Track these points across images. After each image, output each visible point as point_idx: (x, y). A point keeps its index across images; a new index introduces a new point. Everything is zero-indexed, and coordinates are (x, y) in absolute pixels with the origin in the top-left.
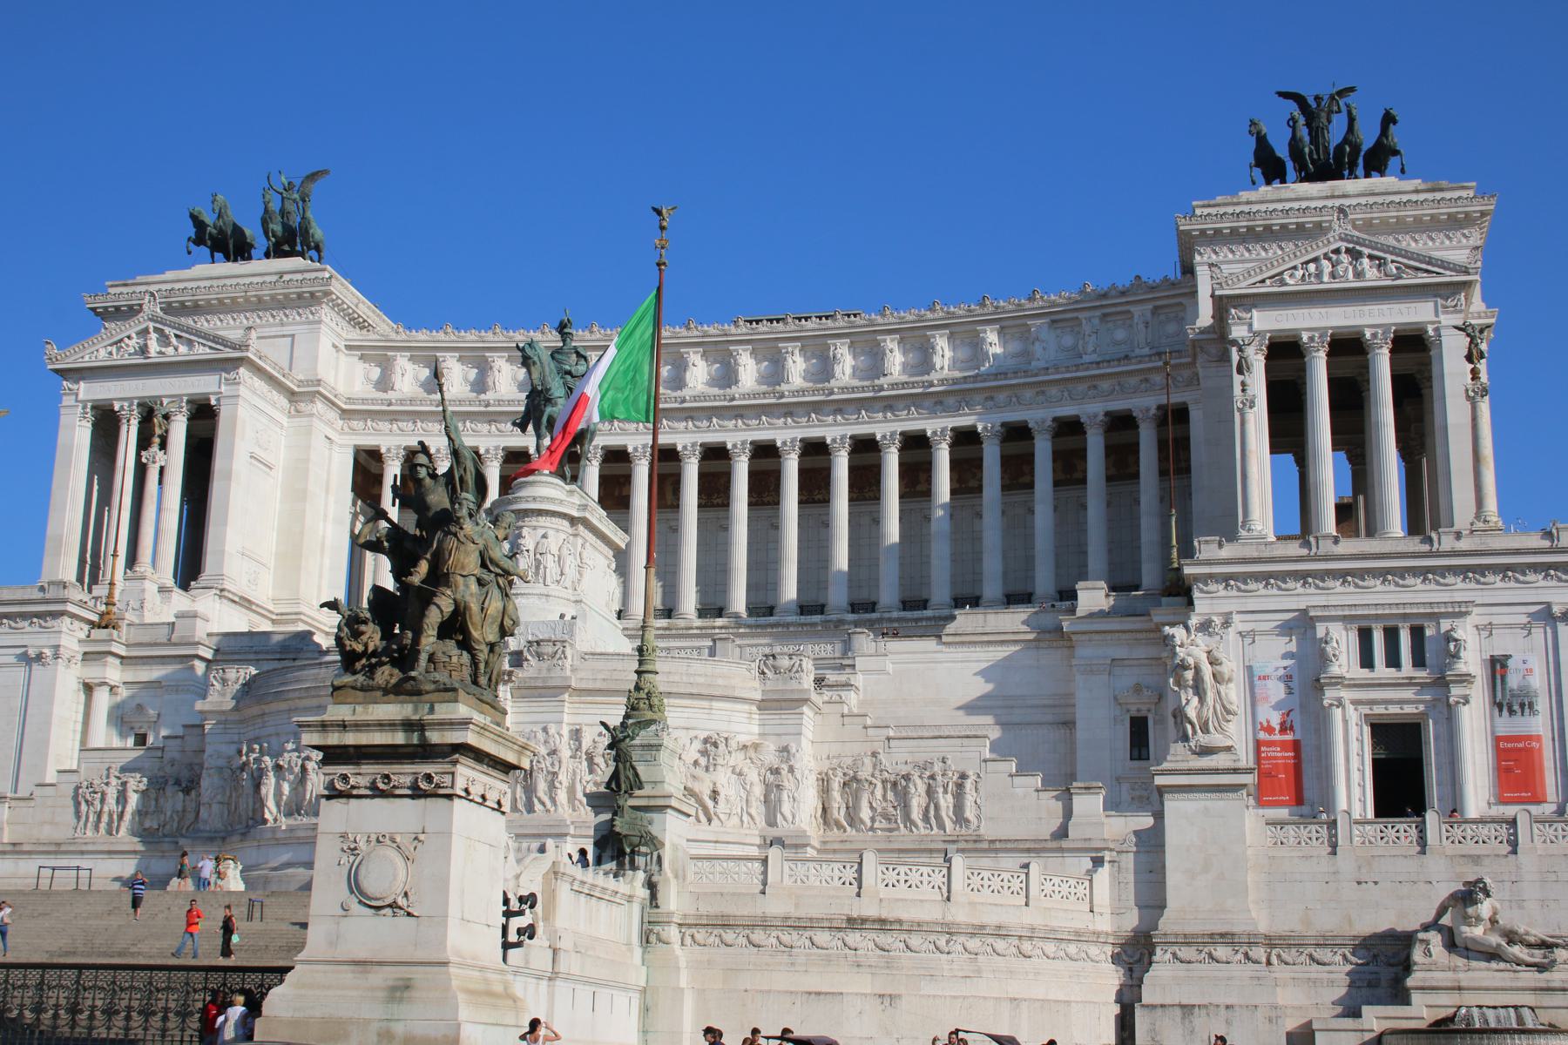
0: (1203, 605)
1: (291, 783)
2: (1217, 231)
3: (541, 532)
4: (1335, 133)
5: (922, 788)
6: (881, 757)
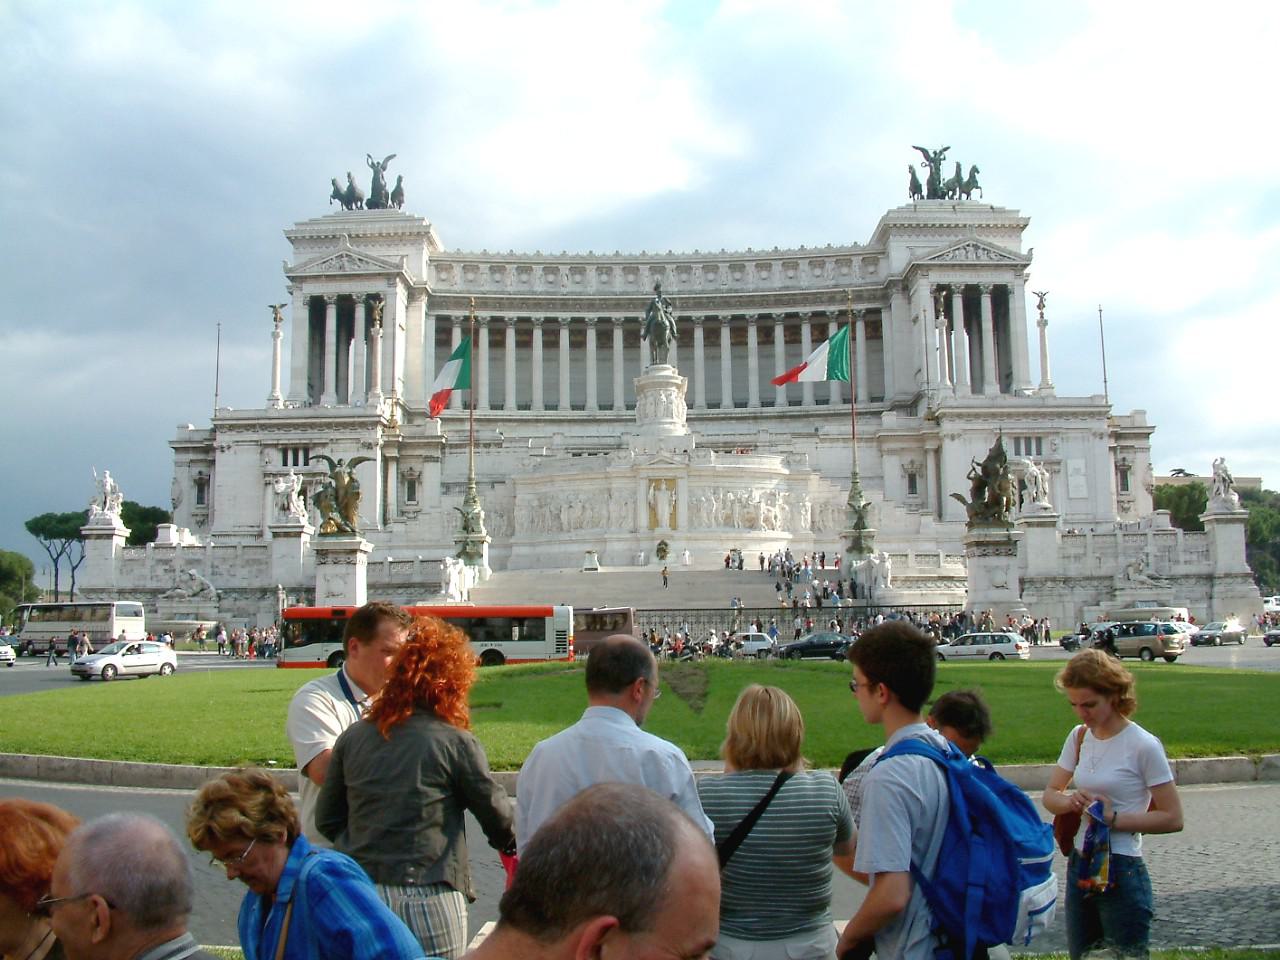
4: (947, 173)
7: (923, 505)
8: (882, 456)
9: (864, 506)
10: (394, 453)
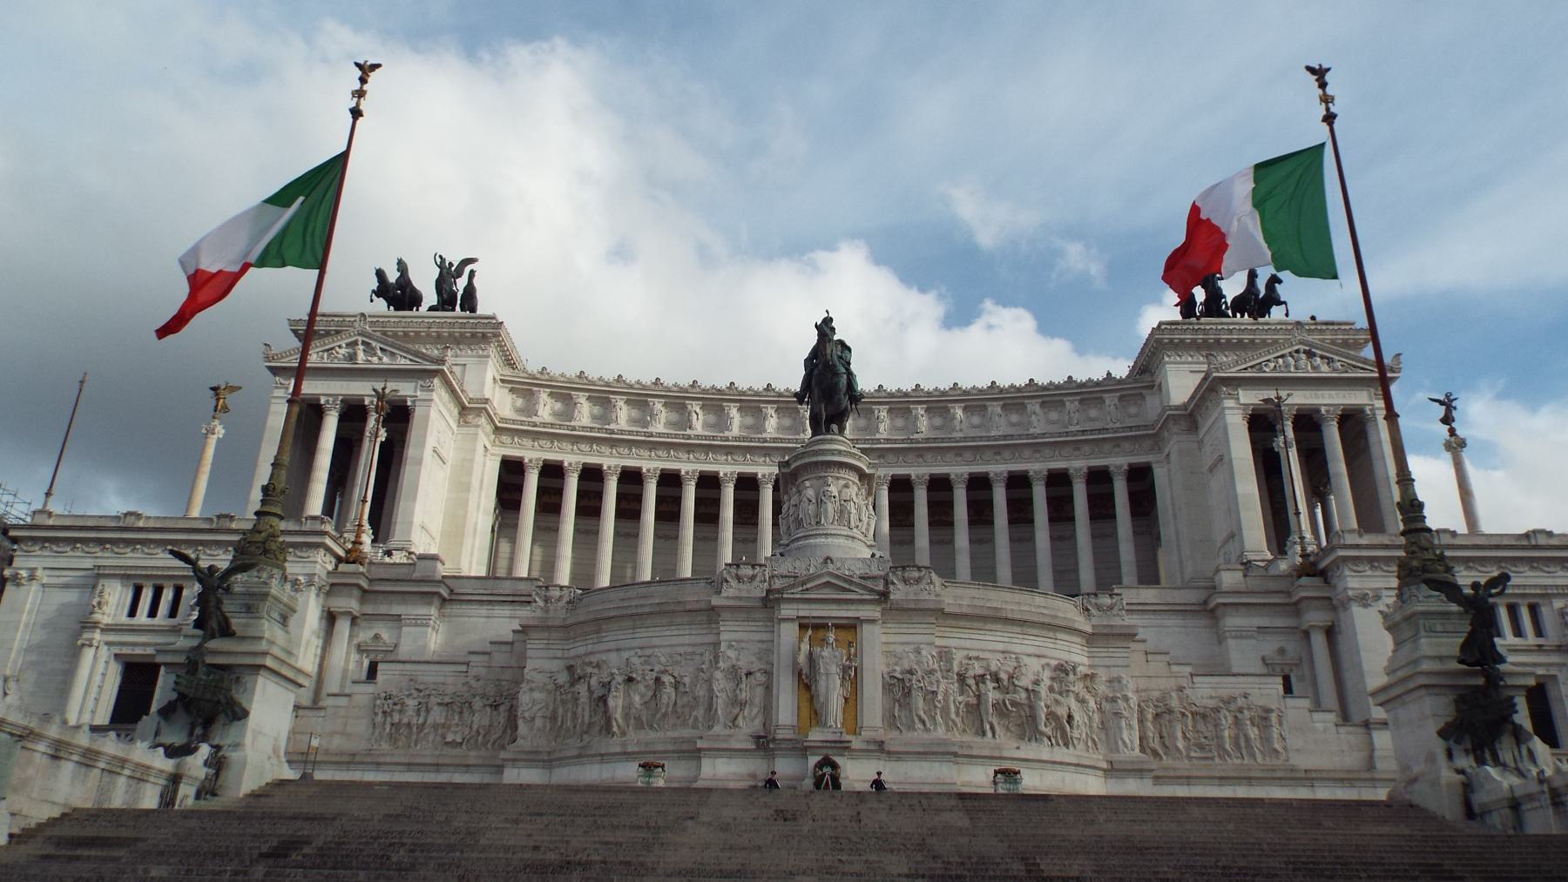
0: (1353, 581)
1: (642, 696)
2: (1182, 341)
3: (842, 482)
5: (1230, 720)
6: (1188, 691)
8: (1220, 643)
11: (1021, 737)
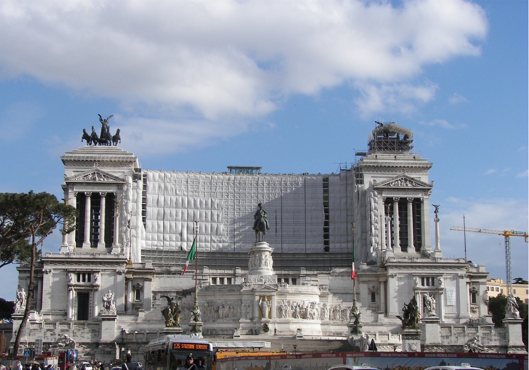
0: (391, 272)
7: (378, 307)
9: (359, 314)
10: (130, 276)
11: (303, 318)
